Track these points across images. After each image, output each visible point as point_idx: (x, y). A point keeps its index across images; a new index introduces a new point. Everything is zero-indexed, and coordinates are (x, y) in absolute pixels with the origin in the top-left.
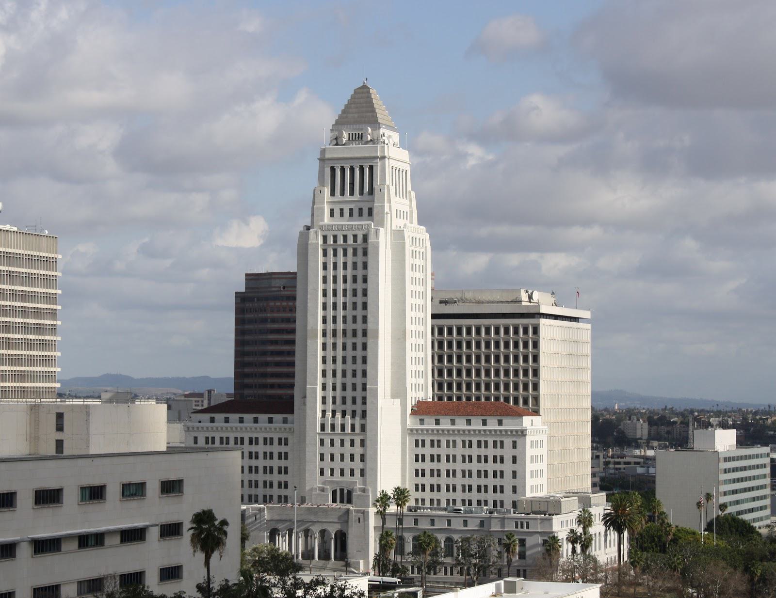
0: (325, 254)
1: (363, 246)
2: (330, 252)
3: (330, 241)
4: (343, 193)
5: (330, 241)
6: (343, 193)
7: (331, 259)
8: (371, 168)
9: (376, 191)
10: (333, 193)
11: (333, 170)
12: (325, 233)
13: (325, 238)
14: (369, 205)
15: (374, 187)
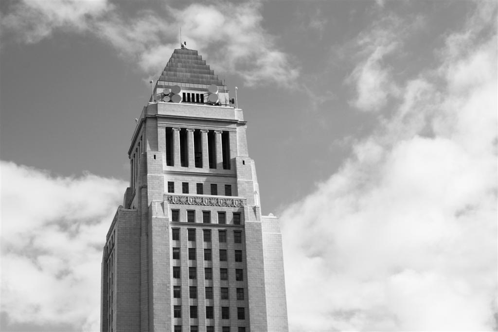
0: (176, 236)
1: (234, 229)
2: (184, 233)
3: (184, 218)
4: (185, 163)
5: (184, 218)
6: (185, 163)
7: (186, 244)
8: (226, 136)
9: (238, 163)
10: (170, 162)
11: (169, 133)
12: (176, 207)
13: (176, 213)
14: (229, 181)
15: (232, 157)
